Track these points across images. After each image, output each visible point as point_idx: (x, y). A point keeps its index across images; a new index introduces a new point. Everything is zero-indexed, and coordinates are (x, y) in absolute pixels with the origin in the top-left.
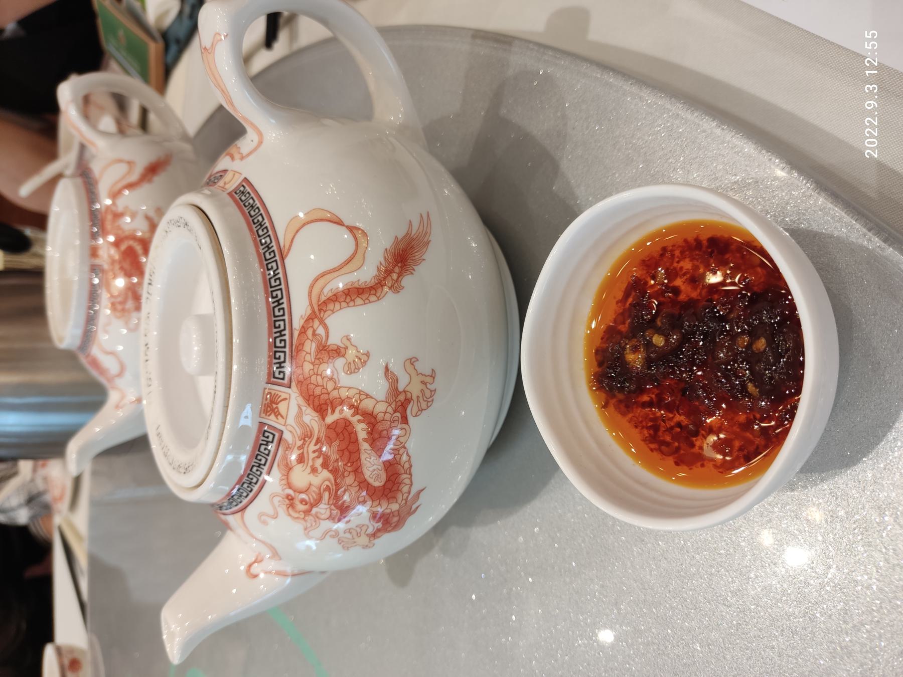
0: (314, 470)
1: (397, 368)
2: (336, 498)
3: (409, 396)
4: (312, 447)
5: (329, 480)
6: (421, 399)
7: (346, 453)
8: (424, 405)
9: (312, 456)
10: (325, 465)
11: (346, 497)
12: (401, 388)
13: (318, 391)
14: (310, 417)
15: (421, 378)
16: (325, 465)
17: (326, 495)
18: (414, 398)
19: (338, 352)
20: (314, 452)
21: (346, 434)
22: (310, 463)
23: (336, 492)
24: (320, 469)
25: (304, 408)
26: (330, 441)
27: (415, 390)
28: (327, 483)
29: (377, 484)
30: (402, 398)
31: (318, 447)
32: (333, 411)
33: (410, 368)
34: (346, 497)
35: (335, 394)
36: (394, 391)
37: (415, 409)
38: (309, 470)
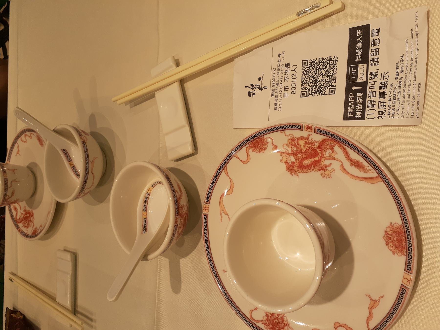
0: (305, 146)
1: (332, 167)
4: (310, 146)
8: (323, 175)
9: (308, 146)
10: (306, 149)
11: (299, 155)
12: (327, 168)
13: (323, 146)
14: (317, 145)
15: (330, 173)
16: (306, 149)
17: (299, 150)
19: (333, 151)
27: (327, 172)
29: (303, 163)
30: (325, 169)
33: (332, 170)
34: (299, 155)
35: (324, 151)
36: (327, 166)
37: (322, 173)
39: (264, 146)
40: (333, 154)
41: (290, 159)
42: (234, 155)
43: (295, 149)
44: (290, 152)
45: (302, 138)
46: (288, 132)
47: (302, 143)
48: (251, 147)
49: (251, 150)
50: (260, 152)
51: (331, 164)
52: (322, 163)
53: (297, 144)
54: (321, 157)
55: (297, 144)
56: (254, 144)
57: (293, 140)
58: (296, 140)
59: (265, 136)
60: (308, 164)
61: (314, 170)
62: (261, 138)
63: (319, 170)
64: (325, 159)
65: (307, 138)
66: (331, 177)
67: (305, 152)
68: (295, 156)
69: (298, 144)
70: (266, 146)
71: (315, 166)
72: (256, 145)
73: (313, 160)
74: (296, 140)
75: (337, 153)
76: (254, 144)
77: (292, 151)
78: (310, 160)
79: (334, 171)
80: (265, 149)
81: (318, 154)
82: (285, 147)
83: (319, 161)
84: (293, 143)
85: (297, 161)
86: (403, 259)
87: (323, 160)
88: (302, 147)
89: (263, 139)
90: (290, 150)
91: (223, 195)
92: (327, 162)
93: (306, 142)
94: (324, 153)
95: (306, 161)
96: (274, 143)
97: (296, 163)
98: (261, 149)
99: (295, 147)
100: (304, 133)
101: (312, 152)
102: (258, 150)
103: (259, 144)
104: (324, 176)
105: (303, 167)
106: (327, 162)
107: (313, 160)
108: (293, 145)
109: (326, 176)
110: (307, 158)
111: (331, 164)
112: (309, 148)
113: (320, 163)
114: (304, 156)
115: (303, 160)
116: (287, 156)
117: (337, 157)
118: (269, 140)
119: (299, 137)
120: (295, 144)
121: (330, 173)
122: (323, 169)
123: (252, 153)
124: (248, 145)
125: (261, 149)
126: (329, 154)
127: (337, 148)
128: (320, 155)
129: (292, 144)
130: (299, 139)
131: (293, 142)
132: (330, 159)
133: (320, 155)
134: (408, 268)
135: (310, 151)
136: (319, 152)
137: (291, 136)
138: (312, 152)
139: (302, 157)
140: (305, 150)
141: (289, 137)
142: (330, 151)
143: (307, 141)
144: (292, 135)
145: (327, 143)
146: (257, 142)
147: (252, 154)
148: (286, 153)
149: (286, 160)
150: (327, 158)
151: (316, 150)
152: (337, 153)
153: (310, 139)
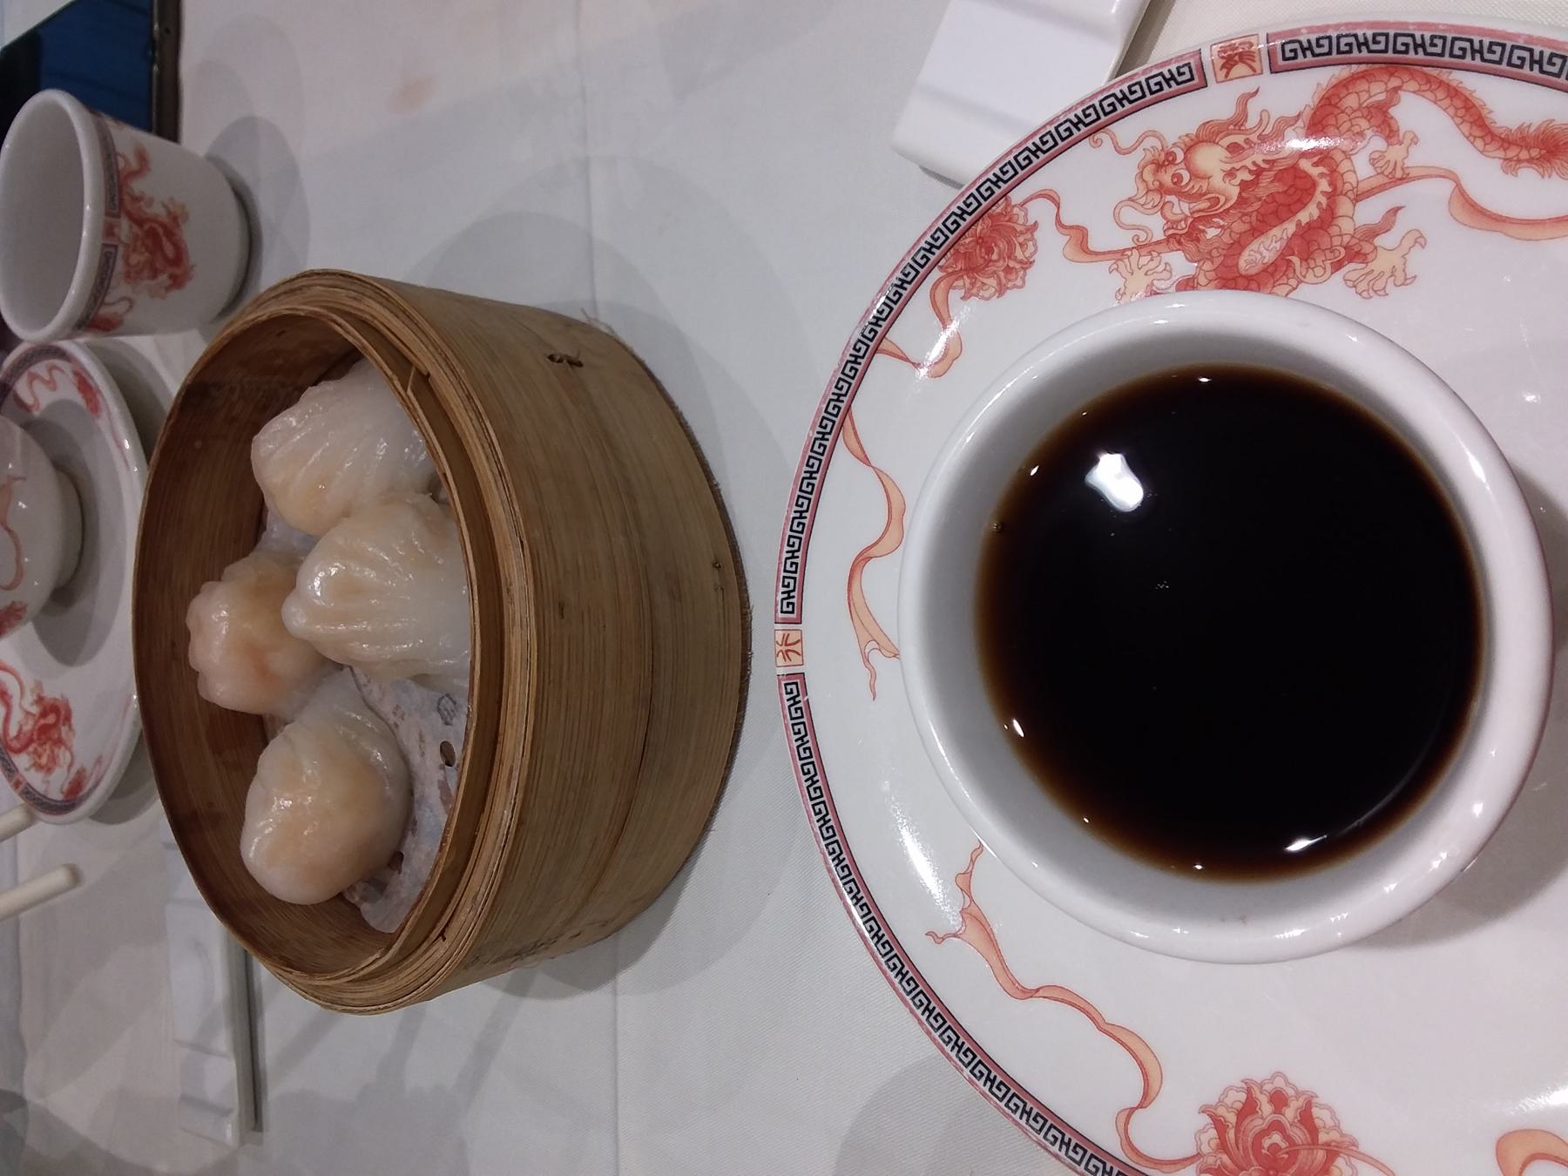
0: (1230, 174)
1: (1403, 224)
2: (1205, 218)
3: (1370, 258)
5: (1227, 200)
6: (1370, 277)
7: (1272, 207)
8: (1362, 286)
9: (1248, 163)
10: (1244, 185)
12: (1378, 241)
15: (1399, 263)
16: (1244, 185)
18: (1371, 266)
20: (1254, 163)
21: (1296, 197)
22: (1237, 166)
23: (1215, 216)
24: (1237, 181)
25: (1300, 123)
26: (1278, 178)
27: (1381, 263)
28: (1222, 199)
30: (1367, 248)
31: (1263, 165)
32: (1316, 164)
33: (1406, 244)
34: (1212, 233)
36: (1372, 233)
38: (1228, 167)
39: (1019, 253)
40: (1395, 153)
41: (1168, 268)
42: (876, 351)
43: (1180, 208)
44: (1159, 235)
45: (1209, 134)
46: (1127, 129)
47: (1211, 160)
48: (952, 276)
49: (955, 295)
50: (1001, 290)
51: (1396, 210)
52: (1346, 226)
53: (1186, 176)
54: (1332, 196)
55: (1186, 176)
56: (967, 256)
57: (1163, 161)
58: (1180, 156)
59: (1017, 196)
60: (1269, 257)
61: (1310, 276)
62: (997, 210)
63: (1337, 266)
64: (1359, 197)
65: (1238, 122)
66: (1407, 281)
67: (1241, 201)
68: (1191, 246)
69: (1195, 176)
70: (1031, 248)
71: (1306, 257)
72: (980, 253)
73: (1290, 228)
74: (1180, 156)
75: (1415, 140)
76: (967, 256)
77: (1171, 224)
78: (1276, 232)
79: (1419, 240)
80: (1027, 264)
81: (1314, 185)
82: (1130, 216)
83: (1329, 216)
84: (1167, 178)
85: (1208, 266)
87: (1344, 206)
88: (1218, 181)
89: (1008, 214)
90: (1156, 227)
92: (1369, 212)
93: (1234, 149)
94: (1344, 166)
95: (1254, 245)
96: (1066, 220)
97: (1202, 280)
98: (1008, 270)
100: (1215, 102)
101: (1277, 187)
102: (992, 282)
103: (990, 251)
104: (1371, 289)
105: (1241, 282)
106: (1369, 212)
107: (1290, 228)
108: (1170, 192)
109: (1379, 285)
110: (1256, 231)
111: (1395, 211)
112: (1258, 172)
113: (1334, 230)
114: (1239, 227)
115: (1238, 245)
116: (1145, 260)
117: (1417, 158)
118: (1040, 212)
119: (1193, 130)
120: (1180, 177)
121: (1399, 263)
122: (1356, 252)
124: (936, 274)
125: (1008, 270)
126: (1373, 162)
127: (1417, 112)
128: (1324, 185)
129: (1162, 190)
130: (1192, 145)
131: (1165, 171)
132: (1382, 188)
133: (1324, 185)
135: (1267, 187)
136: (1315, 172)
137: (1151, 142)
138: (1277, 187)
139: (1227, 239)
140: (1234, 192)
141: (1138, 156)
142: (1378, 143)
143: (1239, 139)
144: (1154, 134)
145: (1351, 101)
146: (981, 241)
147: (966, 312)
148: (1139, 248)
149: (1147, 280)
150: (1364, 186)
151: (1294, 168)
152: (1415, 140)
153: (1252, 122)
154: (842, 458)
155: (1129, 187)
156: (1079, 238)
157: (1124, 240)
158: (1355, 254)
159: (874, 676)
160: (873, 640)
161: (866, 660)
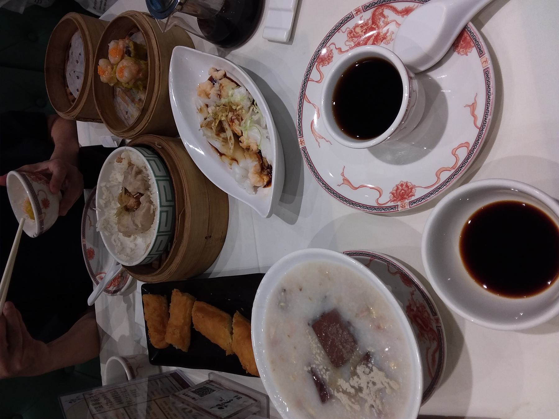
27: (388, 38)
48: (319, 63)
49: (321, 66)
50: (328, 64)
63: (382, 41)
80: (332, 57)
82: (348, 43)
86: (474, 51)
90: (352, 44)
91: (312, 122)
99: (355, 37)
104: (388, 43)
123: (322, 69)
124: (316, 63)
129: (352, 37)
134: (481, 53)
154: (305, 103)
155: (346, 39)
156: (340, 50)
157: (348, 48)
158: (384, 38)
159: (319, 143)
160: (318, 137)
161: (317, 141)
